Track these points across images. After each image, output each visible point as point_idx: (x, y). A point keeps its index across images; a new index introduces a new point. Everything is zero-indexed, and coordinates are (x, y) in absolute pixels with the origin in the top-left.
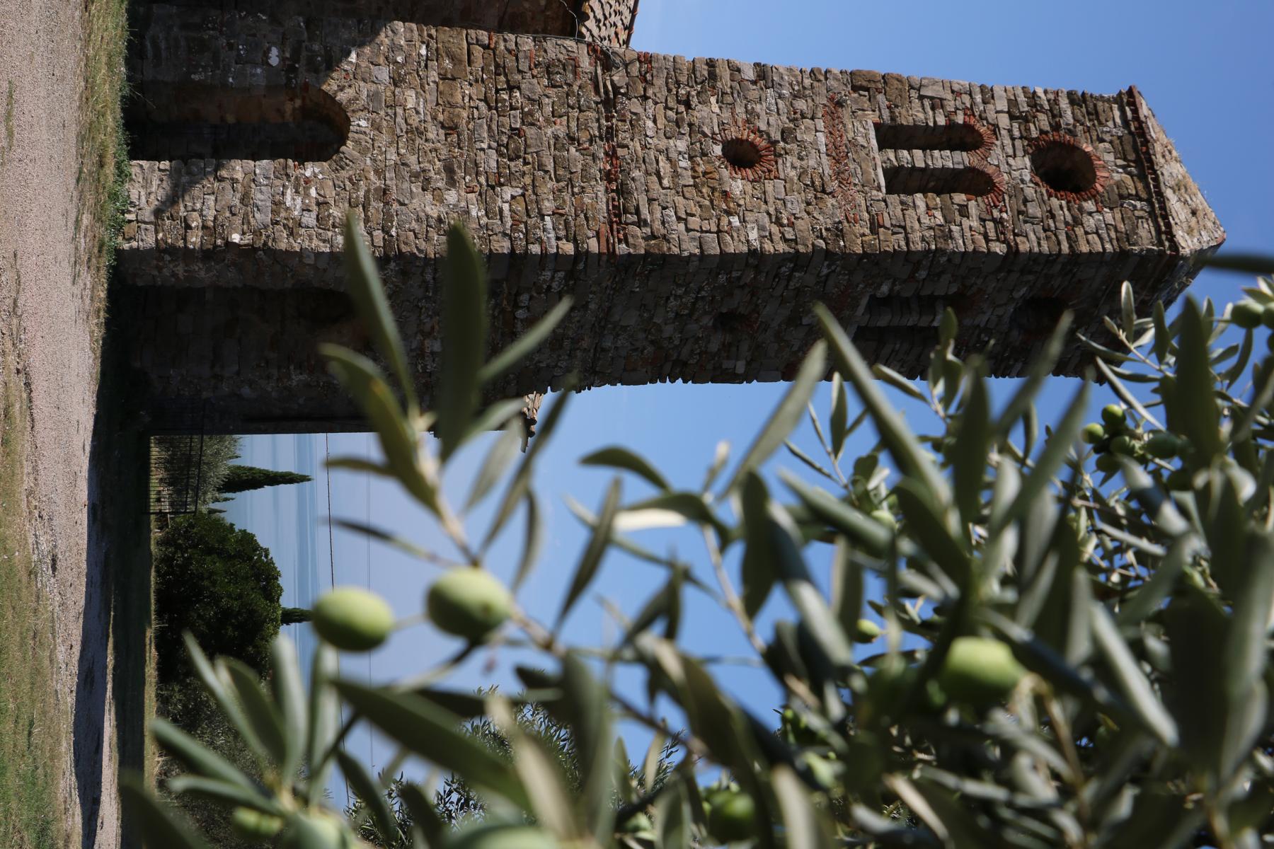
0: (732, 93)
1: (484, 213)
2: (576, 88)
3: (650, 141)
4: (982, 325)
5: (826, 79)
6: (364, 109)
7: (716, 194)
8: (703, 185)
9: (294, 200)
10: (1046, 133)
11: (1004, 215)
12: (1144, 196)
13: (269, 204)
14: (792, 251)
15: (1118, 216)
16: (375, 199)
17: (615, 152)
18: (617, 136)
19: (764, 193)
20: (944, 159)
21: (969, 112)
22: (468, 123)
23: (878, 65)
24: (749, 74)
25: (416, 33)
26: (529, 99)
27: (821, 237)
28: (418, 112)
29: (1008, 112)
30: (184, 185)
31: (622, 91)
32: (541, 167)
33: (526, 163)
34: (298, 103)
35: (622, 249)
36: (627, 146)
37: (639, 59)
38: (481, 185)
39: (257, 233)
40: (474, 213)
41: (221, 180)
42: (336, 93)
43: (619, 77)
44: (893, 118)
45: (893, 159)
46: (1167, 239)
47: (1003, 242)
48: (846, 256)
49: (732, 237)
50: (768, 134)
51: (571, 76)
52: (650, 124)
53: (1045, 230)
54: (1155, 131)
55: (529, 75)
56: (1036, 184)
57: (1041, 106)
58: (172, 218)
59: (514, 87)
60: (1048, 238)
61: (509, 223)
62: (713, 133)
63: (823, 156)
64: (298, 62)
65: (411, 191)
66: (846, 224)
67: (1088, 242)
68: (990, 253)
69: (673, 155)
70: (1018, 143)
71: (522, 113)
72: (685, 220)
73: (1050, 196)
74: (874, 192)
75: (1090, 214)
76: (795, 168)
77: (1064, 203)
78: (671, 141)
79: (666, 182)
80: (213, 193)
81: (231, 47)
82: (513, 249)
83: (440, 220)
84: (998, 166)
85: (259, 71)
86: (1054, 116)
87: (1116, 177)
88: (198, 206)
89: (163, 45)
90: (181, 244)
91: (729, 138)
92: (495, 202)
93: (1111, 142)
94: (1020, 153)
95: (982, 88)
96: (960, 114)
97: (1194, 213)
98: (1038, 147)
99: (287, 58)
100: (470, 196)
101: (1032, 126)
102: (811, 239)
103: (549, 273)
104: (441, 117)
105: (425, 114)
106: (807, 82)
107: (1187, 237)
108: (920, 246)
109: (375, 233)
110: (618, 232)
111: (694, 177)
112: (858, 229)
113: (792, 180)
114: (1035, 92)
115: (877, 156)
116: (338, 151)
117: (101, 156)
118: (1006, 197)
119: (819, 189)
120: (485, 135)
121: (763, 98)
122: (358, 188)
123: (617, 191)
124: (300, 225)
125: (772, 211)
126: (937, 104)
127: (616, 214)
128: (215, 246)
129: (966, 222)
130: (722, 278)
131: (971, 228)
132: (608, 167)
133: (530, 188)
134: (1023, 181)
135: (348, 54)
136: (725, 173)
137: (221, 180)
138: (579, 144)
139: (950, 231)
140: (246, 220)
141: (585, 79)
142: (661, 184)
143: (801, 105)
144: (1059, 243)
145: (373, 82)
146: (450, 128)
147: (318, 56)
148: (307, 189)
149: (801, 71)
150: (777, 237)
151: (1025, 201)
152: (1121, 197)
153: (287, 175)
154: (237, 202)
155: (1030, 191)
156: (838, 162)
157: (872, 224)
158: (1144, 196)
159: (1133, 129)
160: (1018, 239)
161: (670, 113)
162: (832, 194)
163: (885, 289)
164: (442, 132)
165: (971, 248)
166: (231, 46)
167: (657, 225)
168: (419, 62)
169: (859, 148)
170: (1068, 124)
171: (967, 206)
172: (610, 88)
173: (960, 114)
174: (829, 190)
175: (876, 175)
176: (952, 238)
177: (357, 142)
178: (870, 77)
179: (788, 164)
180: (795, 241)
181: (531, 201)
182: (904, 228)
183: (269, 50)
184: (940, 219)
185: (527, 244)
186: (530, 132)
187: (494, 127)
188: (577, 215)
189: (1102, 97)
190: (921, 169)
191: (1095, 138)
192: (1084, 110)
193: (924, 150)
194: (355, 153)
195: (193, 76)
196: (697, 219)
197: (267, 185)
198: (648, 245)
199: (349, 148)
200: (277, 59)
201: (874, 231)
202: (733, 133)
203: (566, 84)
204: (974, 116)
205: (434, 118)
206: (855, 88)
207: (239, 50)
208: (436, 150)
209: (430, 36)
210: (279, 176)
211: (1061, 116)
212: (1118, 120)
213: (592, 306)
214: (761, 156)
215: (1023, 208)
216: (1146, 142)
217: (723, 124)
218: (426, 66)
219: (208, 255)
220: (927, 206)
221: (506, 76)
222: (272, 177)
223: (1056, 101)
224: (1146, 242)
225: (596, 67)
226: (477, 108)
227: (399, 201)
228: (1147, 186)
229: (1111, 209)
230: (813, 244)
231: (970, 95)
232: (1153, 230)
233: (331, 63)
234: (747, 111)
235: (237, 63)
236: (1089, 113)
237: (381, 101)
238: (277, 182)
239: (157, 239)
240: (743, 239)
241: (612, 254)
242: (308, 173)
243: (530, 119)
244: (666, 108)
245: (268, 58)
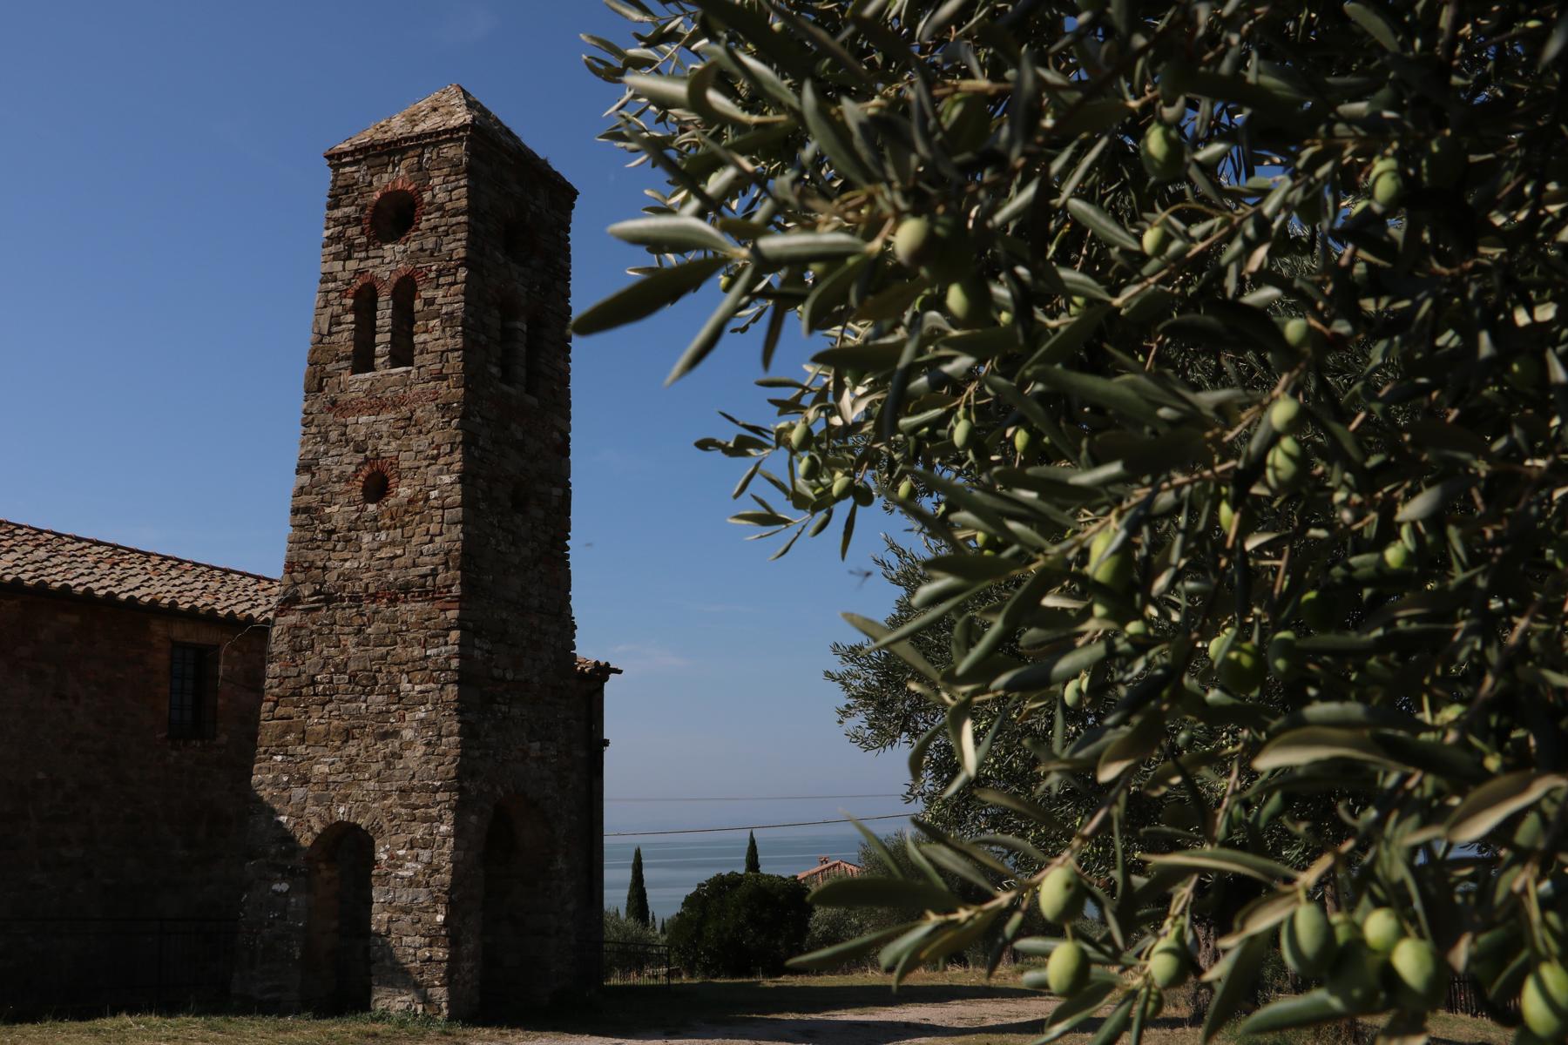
0: (322, 494)
2: (315, 627)
3: (362, 564)
4: (526, 290)
5: (311, 413)
6: (329, 808)
7: (410, 509)
8: (402, 521)
9: (408, 869)
10: (363, 229)
11: (434, 268)
12: (420, 150)
13: (411, 890)
14: (461, 447)
15: (436, 173)
17: (372, 595)
18: (358, 593)
19: (410, 469)
20: (384, 315)
21: (343, 294)
22: (343, 720)
23: (301, 368)
24: (305, 479)
25: (262, 764)
26: (323, 667)
27: (450, 422)
28: (333, 763)
29: (344, 260)
31: (318, 587)
32: (383, 657)
33: (380, 671)
34: (322, 866)
35: (456, 590)
36: (367, 585)
37: (290, 573)
38: (398, 709)
39: (436, 900)
40: (423, 715)
41: (389, 931)
42: (314, 833)
43: (306, 591)
44: (347, 358)
45: (383, 360)
46: (457, 133)
47: (457, 270)
48: (466, 402)
49: (448, 497)
50: (359, 464)
51: (303, 632)
52: (347, 564)
53: (448, 235)
54: (364, 139)
55: (302, 668)
56: (408, 240)
57: (340, 232)
58: (421, 973)
59: (313, 680)
60: (454, 233)
61: (432, 685)
62: (357, 511)
63: (379, 418)
66: (439, 401)
67: (457, 199)
68: (467, 281)
69: (376, 545)
70: (371, 254)
71: (335, 673)
72: (432, 536)
73: (418, 229)
74: (412, 376)
75: (434, 196)
76: (389, 442)
78: (364, 547)
79: (399, 552)
82: (455, 682)
83: (428, 744)
84: (391, 272)
85: (293, 900)
86: (349, 222)
87: (402, 173)
88: (411, 951)
90: (444, 965)
91: (361, 497)
92: (413, 697)
93: (372, 176)
94: (380, 253)
95: (322, 282)
96: (344, 301)
97: (435, 109)
98: (375, 237)
101: (356, 241)
102: (450, 431)
103: (476, 652)
104: (338, 743)
105: (335, 756)
106: (314, 430)
107: (456, 116)
108: (459, 340)
109: (438, 799)
110: (442, 593)
111: (395, 528)
112: (443, 391)
113: (399, 445)
114: (327, 238)
115: (380, 373)
116: (366, 832)
117: (368, 1036)
118: (418, 266)
119: (408, 422)
120: (354, 705)
121: (327, 467)
123: (406, 594)
124: (430, 863)
125: (425, 463)
126: (335, 321)
127: (426, 594)
128: (446, 936)
129: (439, 300)
130: (483, 506)
131: (443, 297)
132: (385, 600)
133: (401, 667)
134: (405, 251)
135: (280, 823)
136: (392, 501)
137: (389, 931)
138: (364, 625)
139: (446, 314)
140: (425, 910)
141: (307, 619)
142: (400, 556)
143: (334, 436)
144: (459, 223)
145: (305, 801)
146: (347, 735)
148: (399, 858)
149: (304, 435)
150: (449, 459)
151: (422, 250)
152: (420, 169)
153: (386, 875)
154: (408, 918)
155: (414, 246)
156: (384, 406)
157: (439, 379)
158: (420, 150)
159: (361, 157)
160: (455, 257)
161: (338, 547)
162: (412, 412)
163: (494, 370)
164: (350, 742)
165: (462, 297)
167: (436, 560)
168: (289, 762)
169: (373, 388)
170: (356, 211)
171: (425, 299)
173: (344, 301)
174: (409, 415)
175: (396, 374)
176: (453, 313)
177: (358, 815)
178: (311, 376)
179: (386, 448)
180: (452, 444)
181: (413, 666)
182: (443, 352)
183: (274, 891)
184: (436, 322)
185: (450, 670)
186: (352, 666)
187: (348, 697)
188: (427, 628)
189: (332, 182)
190: (392, 337)
191: (368, 189)
192: (344, 197)
193: (376, 333)
196: (432, 527)
198: (453, 568)
199: (363, 822)
200: (284, 884)
201: (445, 378)
202: (357, 494)
203: (311, 635)
204: (347, 290)
205: (338, 749)
206: (321, 389)
207: (274, 917)
208: (367, 747)
209: (265, 752)
211: (349, 217)
212: (354, 169)
213: (504, 615)
214: (378, 470)
215: (428, 252)
216: (373, 146)
217: (349, 502)
218: (292, 756)
219: (454, 942)
220: (424, 332)
221: (302, 687)
223: (336, 220)
224: (459, 151)
225: (296, 610)
226: (330, 712)
227: (411, 779)
228: (411, 148)
229: (430, 178)
230: (455, 429)
231: (329, 292)
232: (448, 145)
233: (288, 838)
234: (339, 482)
235: (286, 920)
236: (347, 193)
238: (392, 883)
239: (441, 986)
240: (450, 488)
241: (460, 598)
242: (385, 857)
243: (341, 667)
244: (334, 550)
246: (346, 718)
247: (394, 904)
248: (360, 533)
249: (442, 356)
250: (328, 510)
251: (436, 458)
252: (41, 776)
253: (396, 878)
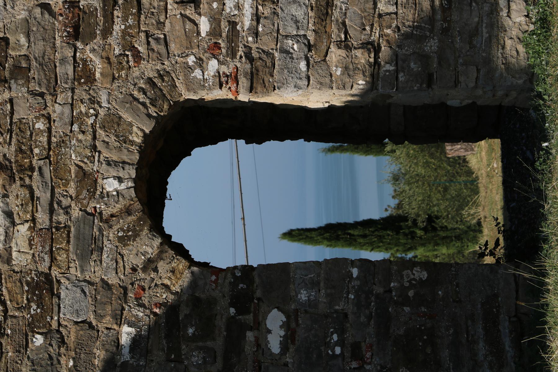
6: (107, 221)
16: (93, 13)
30: (432, 31)
64: (231, 320)
65: (28, 36)
80: (380, 16)
85: (303, 296)
89: (482, 348)
99: (251, 329)
122: (123, 37)
135: (136, 341)
145: (90, 283)
147: (195, 338)
148: (215, 32)
194: (127, 117)
197: (287, 37)
200: (269, 325)
207: (341, 343)
210: (264, 56)
222: (277, 55)
227: (52, 13)
237: (77, 238)
238: (268, 43)
245: (286, 326)
247: (311, 37)
253: (256, 34)
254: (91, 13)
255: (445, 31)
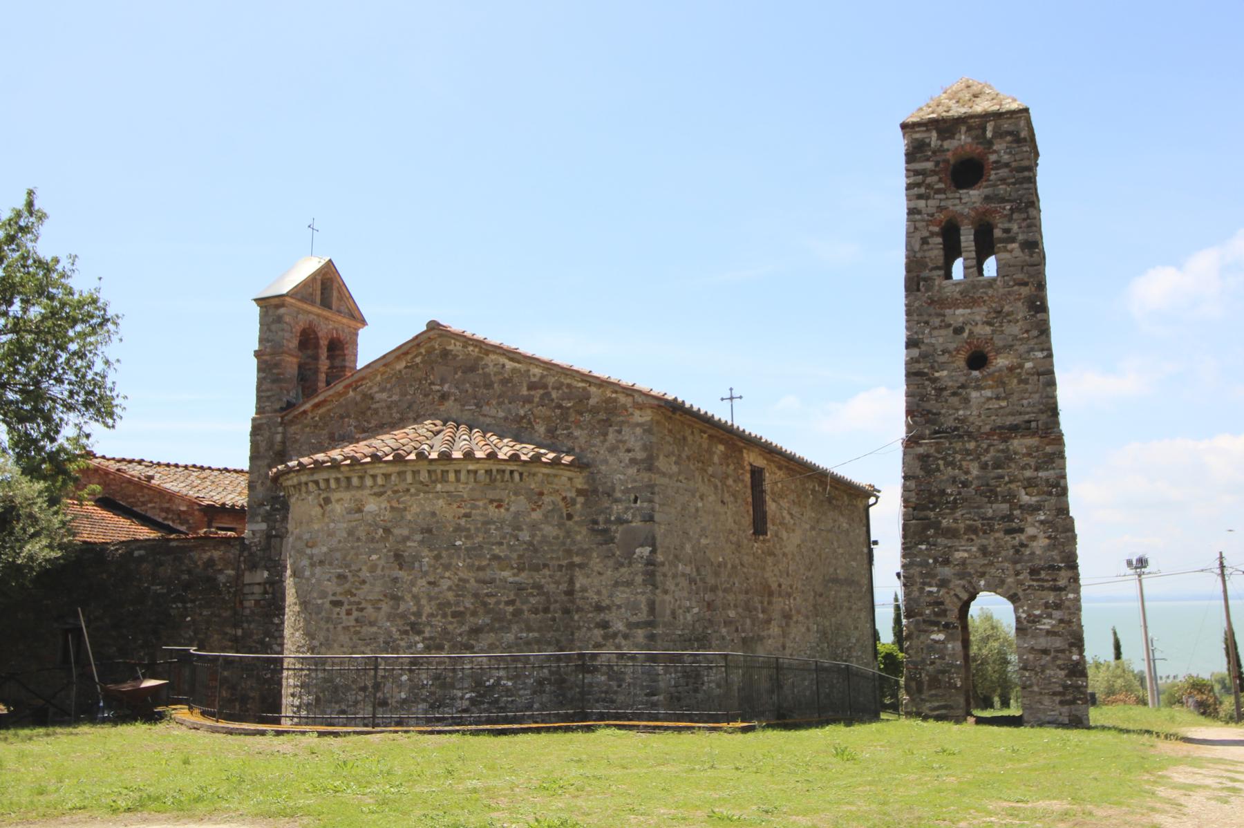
1: (1041, 512)
2: (939, 456)
11: (1008, 207)
21: (929, 223)
24: (915, 352)
52: (961, 412)
56: (980, 187)
72: (1031, 393)
73: (988, 180)
77: (993, 172)
81: (932, 663)
83: (1049, 537)
89: (936, 704)
100: (1030, 519)
101: (936, 187)
126: (924, 241)
136: (992, 369)
148: (1036, 616)
155: (988, 191)
160: (1025, 200)
162: (1002, 307)
166: (932, 663)
172: (938, 435)
183: (933, 640)
195: (958, 686)
201: (1026, 284)
207: (935, 658)
226: (962, 515)
234: (943, 354)
245: (939, 640)
246: (976, 518)
248: (968, 390)
249: (1022, 269)
250: (937, 374)
251: (1028, 339)
252: (721, 559)
254: (1039, 574)
255: (1041, 693)
